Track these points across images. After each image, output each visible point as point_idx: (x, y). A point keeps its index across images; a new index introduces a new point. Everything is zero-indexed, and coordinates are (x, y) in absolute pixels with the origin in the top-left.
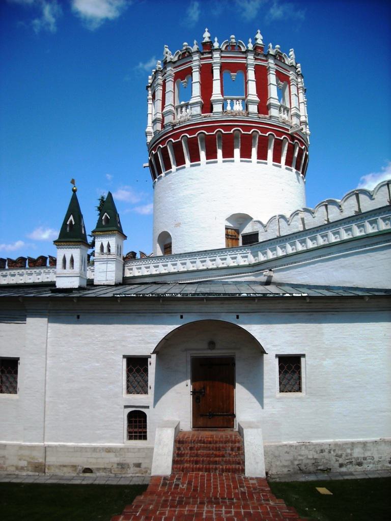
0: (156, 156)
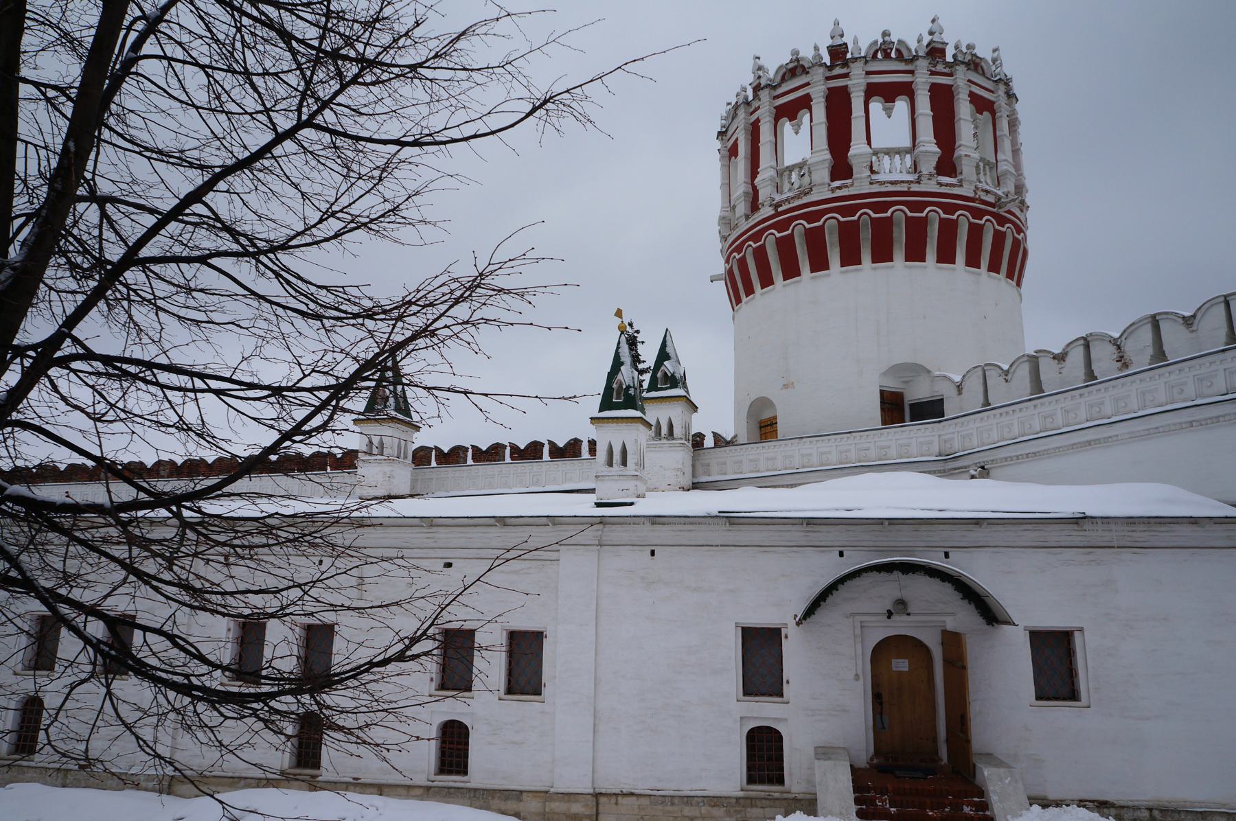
0: (742, 263)
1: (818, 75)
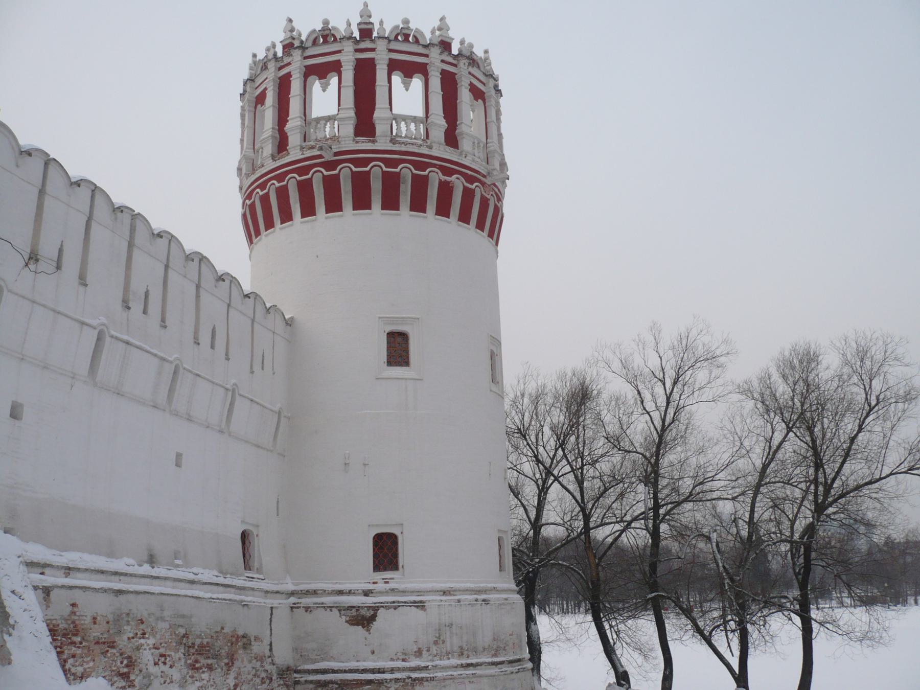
1: (349, 47)
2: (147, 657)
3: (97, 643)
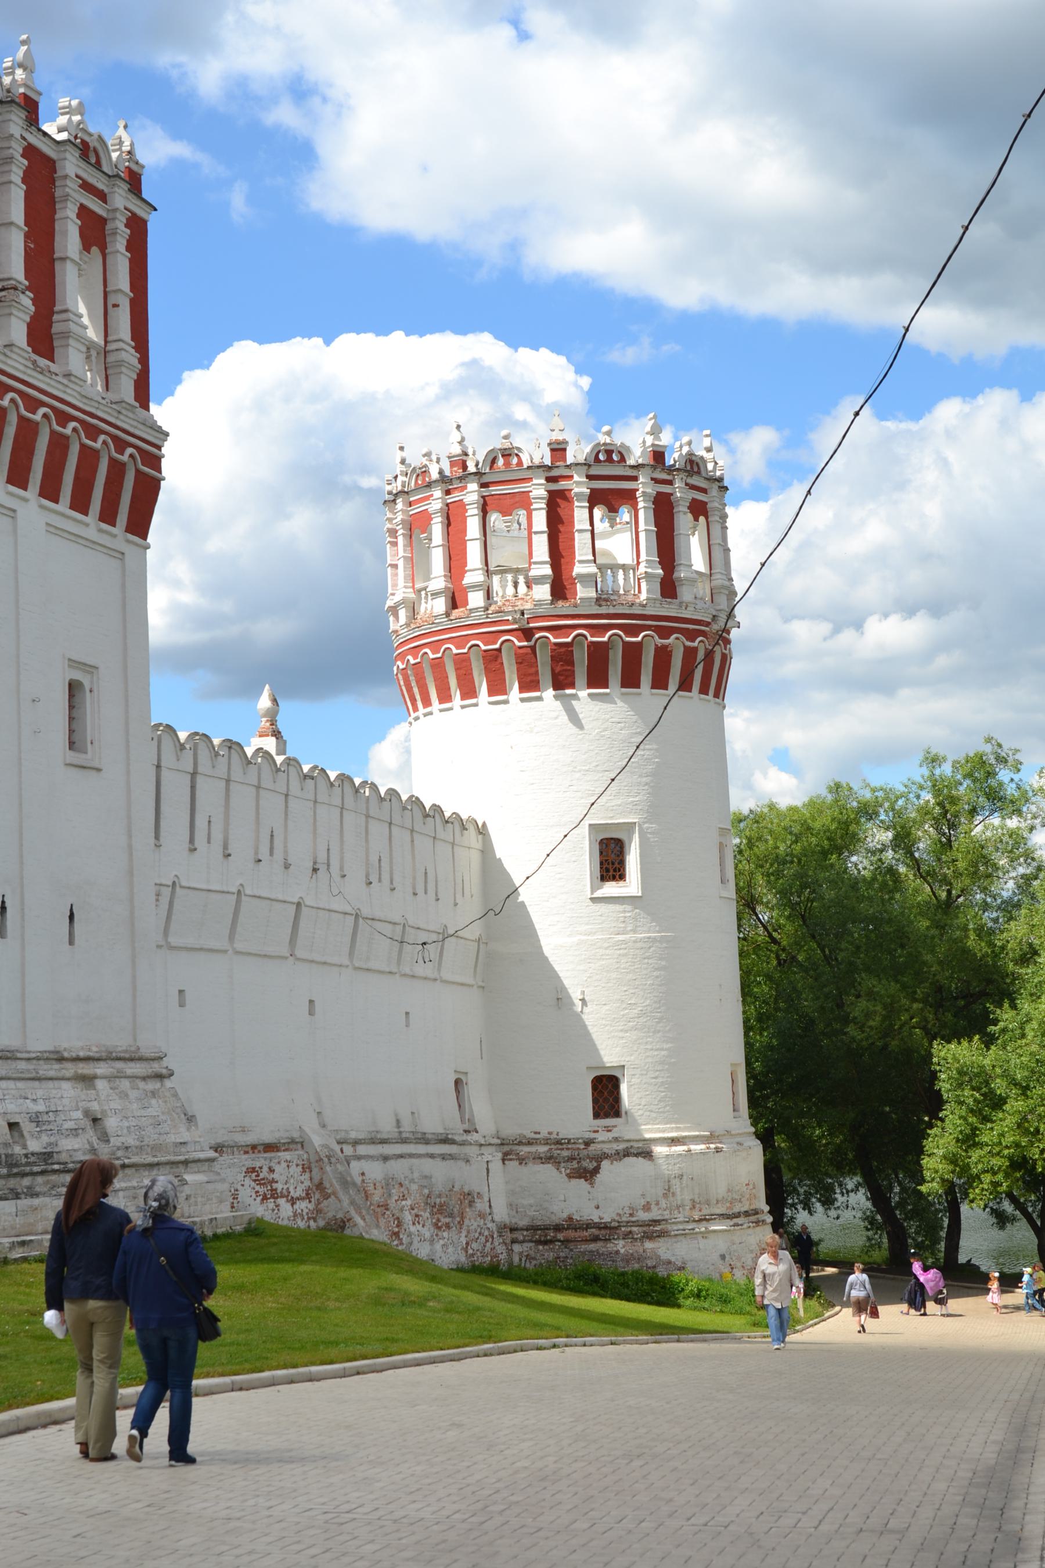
2: (408, 1217)
3: (379, 1206)
